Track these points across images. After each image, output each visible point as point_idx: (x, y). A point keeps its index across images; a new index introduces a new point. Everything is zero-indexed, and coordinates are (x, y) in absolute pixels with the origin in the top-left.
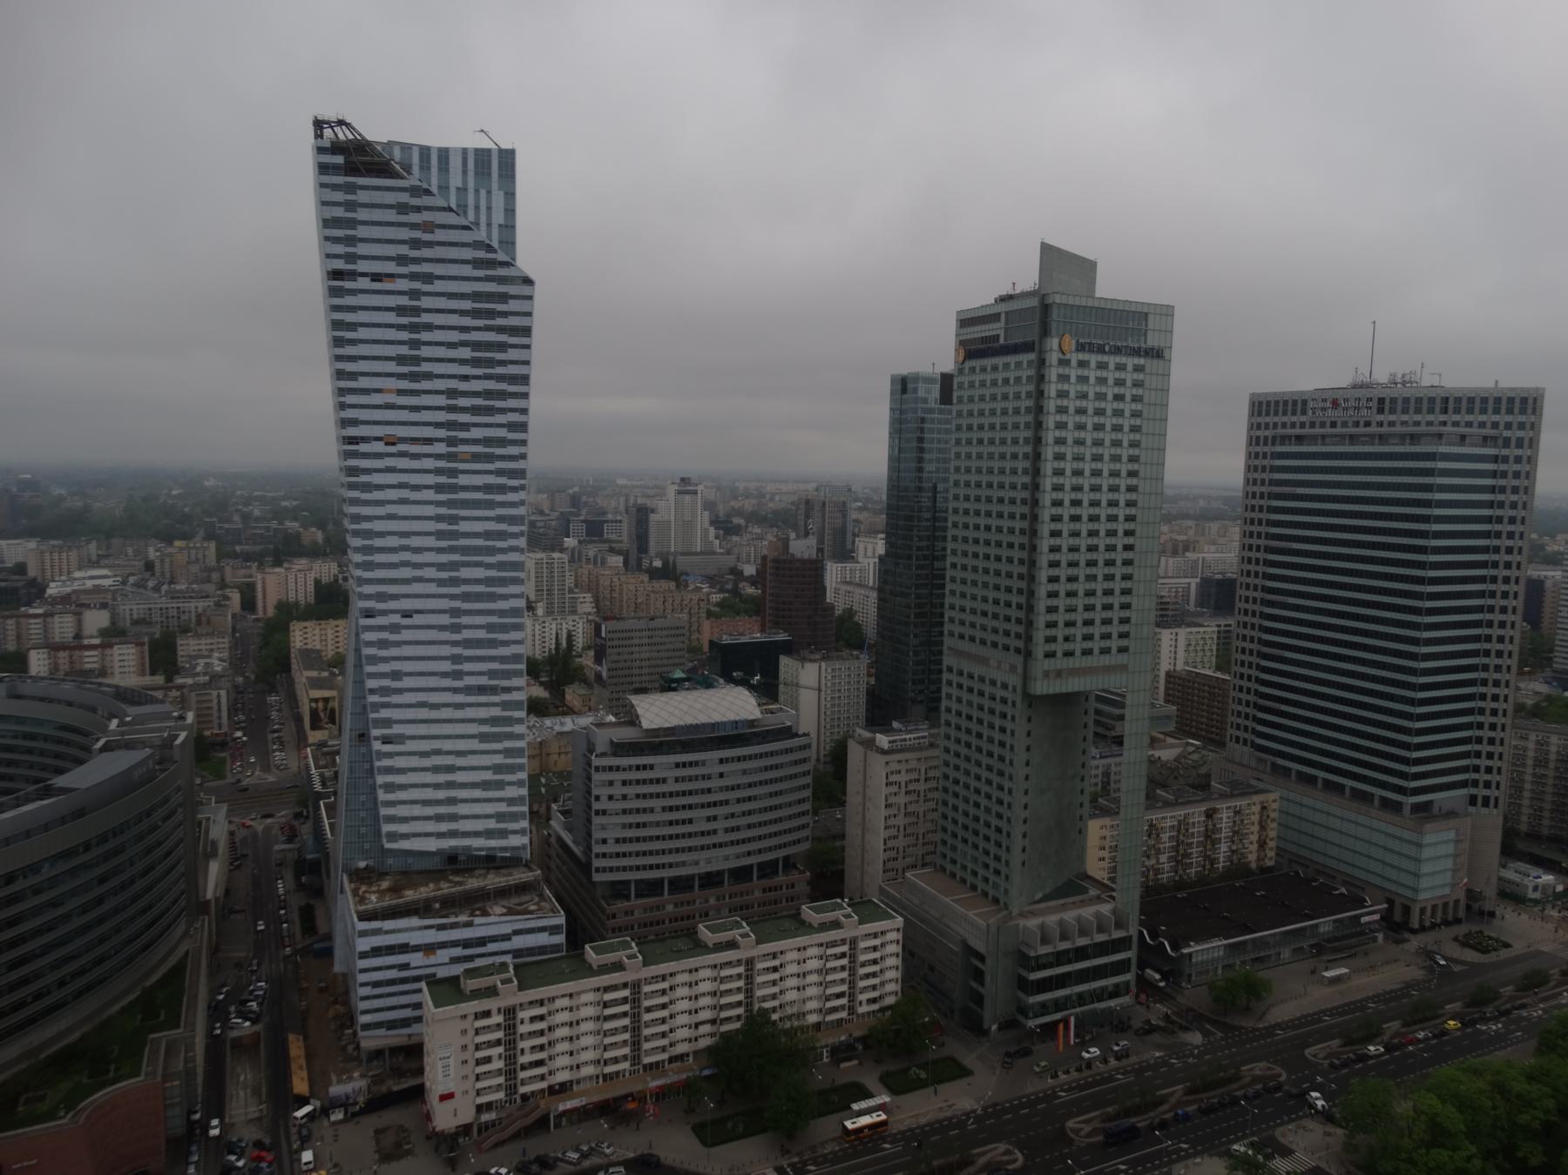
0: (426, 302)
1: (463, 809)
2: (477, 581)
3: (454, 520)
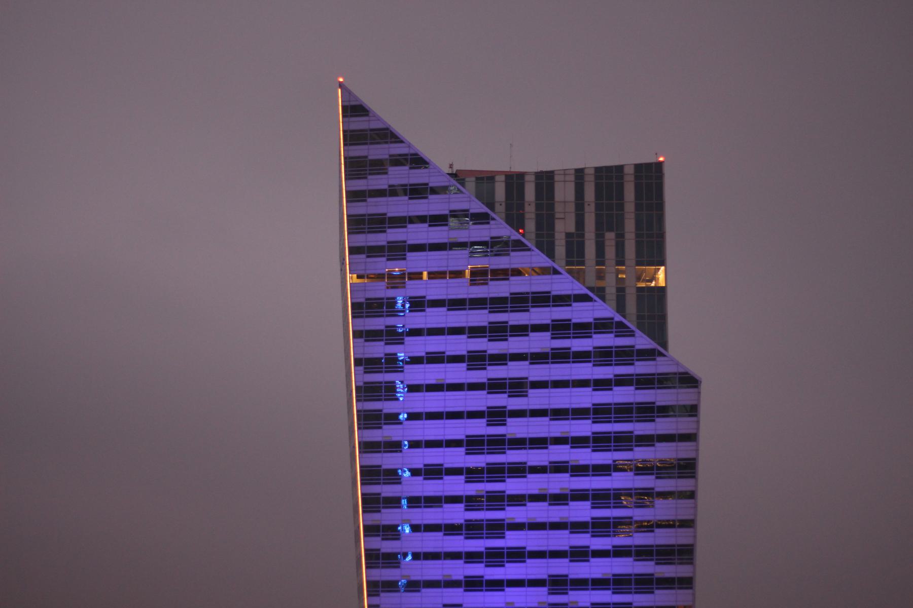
0: (515, 428)
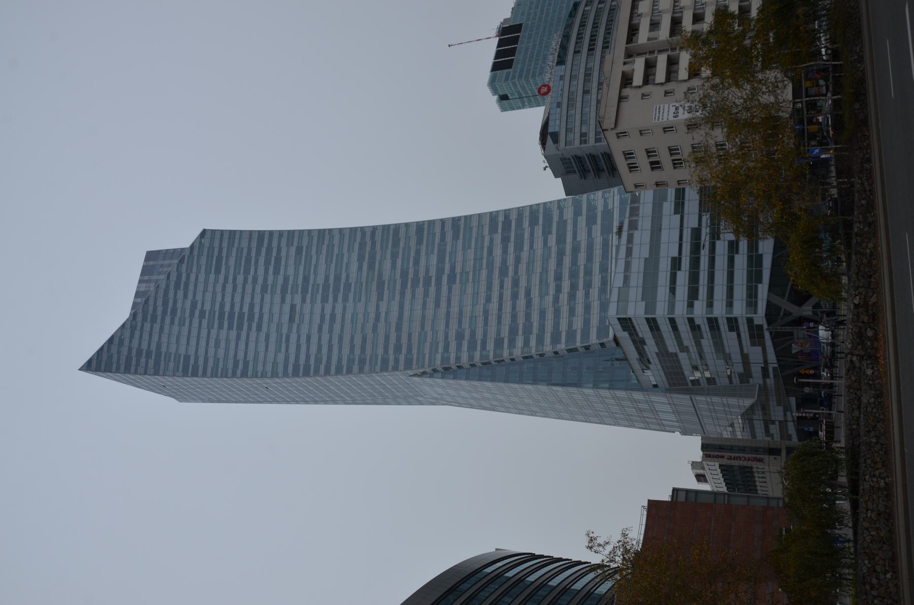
0: (207, 307)
2: (394, 266)
3: (348, 286)
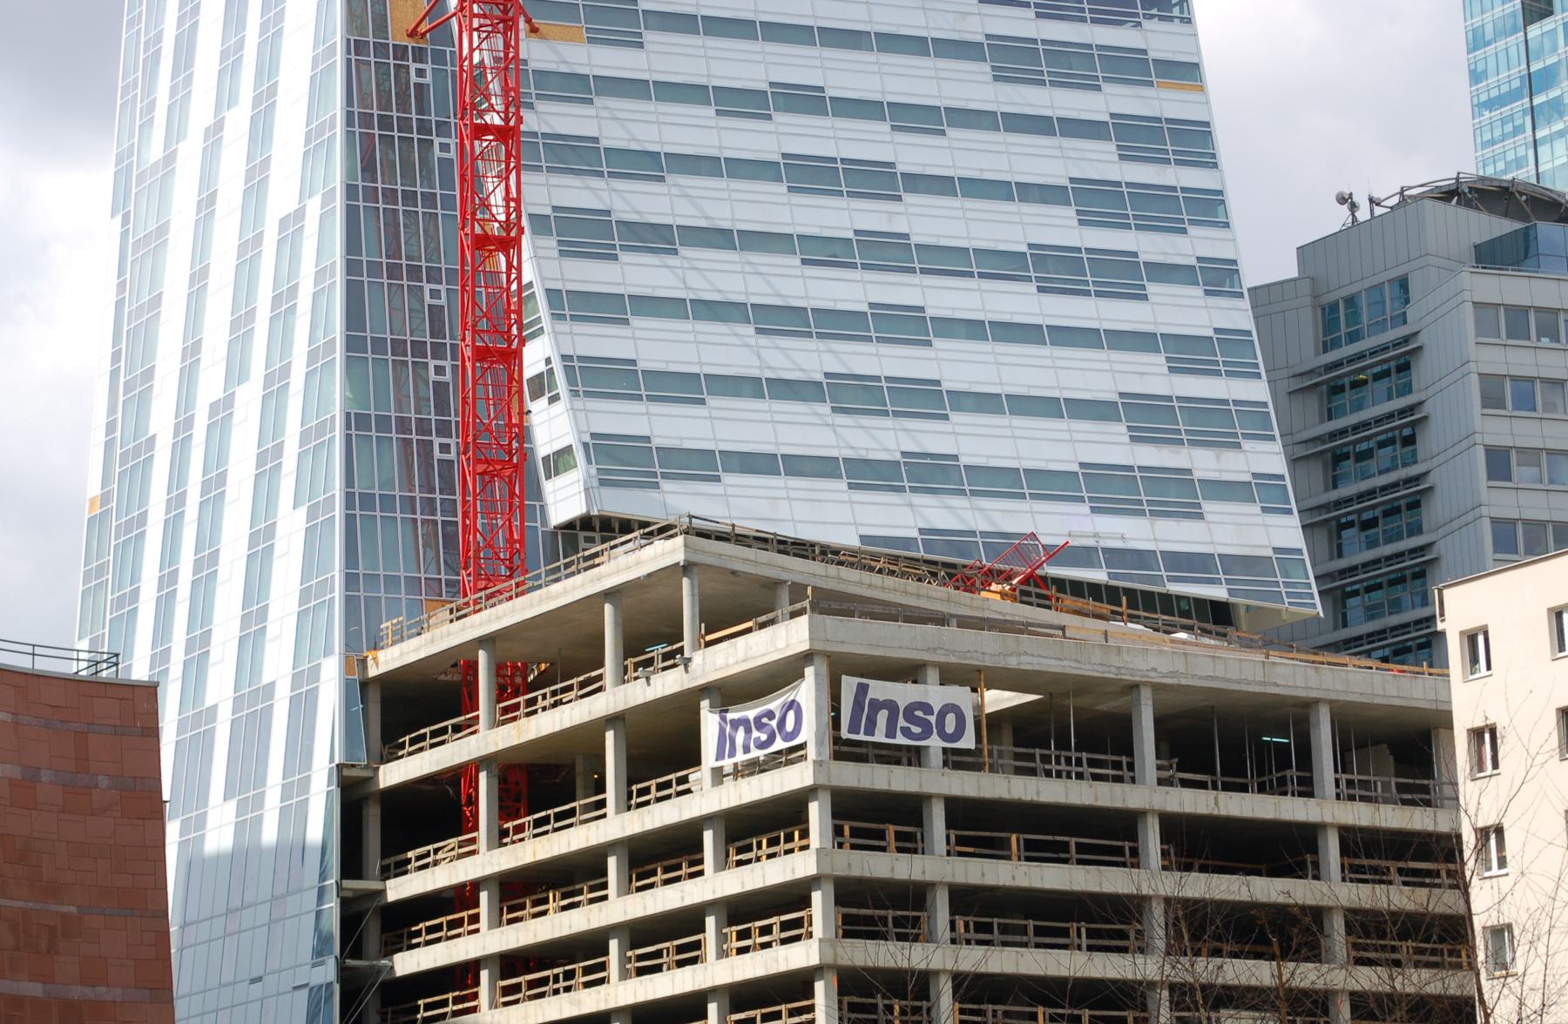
1: (956, 365)
